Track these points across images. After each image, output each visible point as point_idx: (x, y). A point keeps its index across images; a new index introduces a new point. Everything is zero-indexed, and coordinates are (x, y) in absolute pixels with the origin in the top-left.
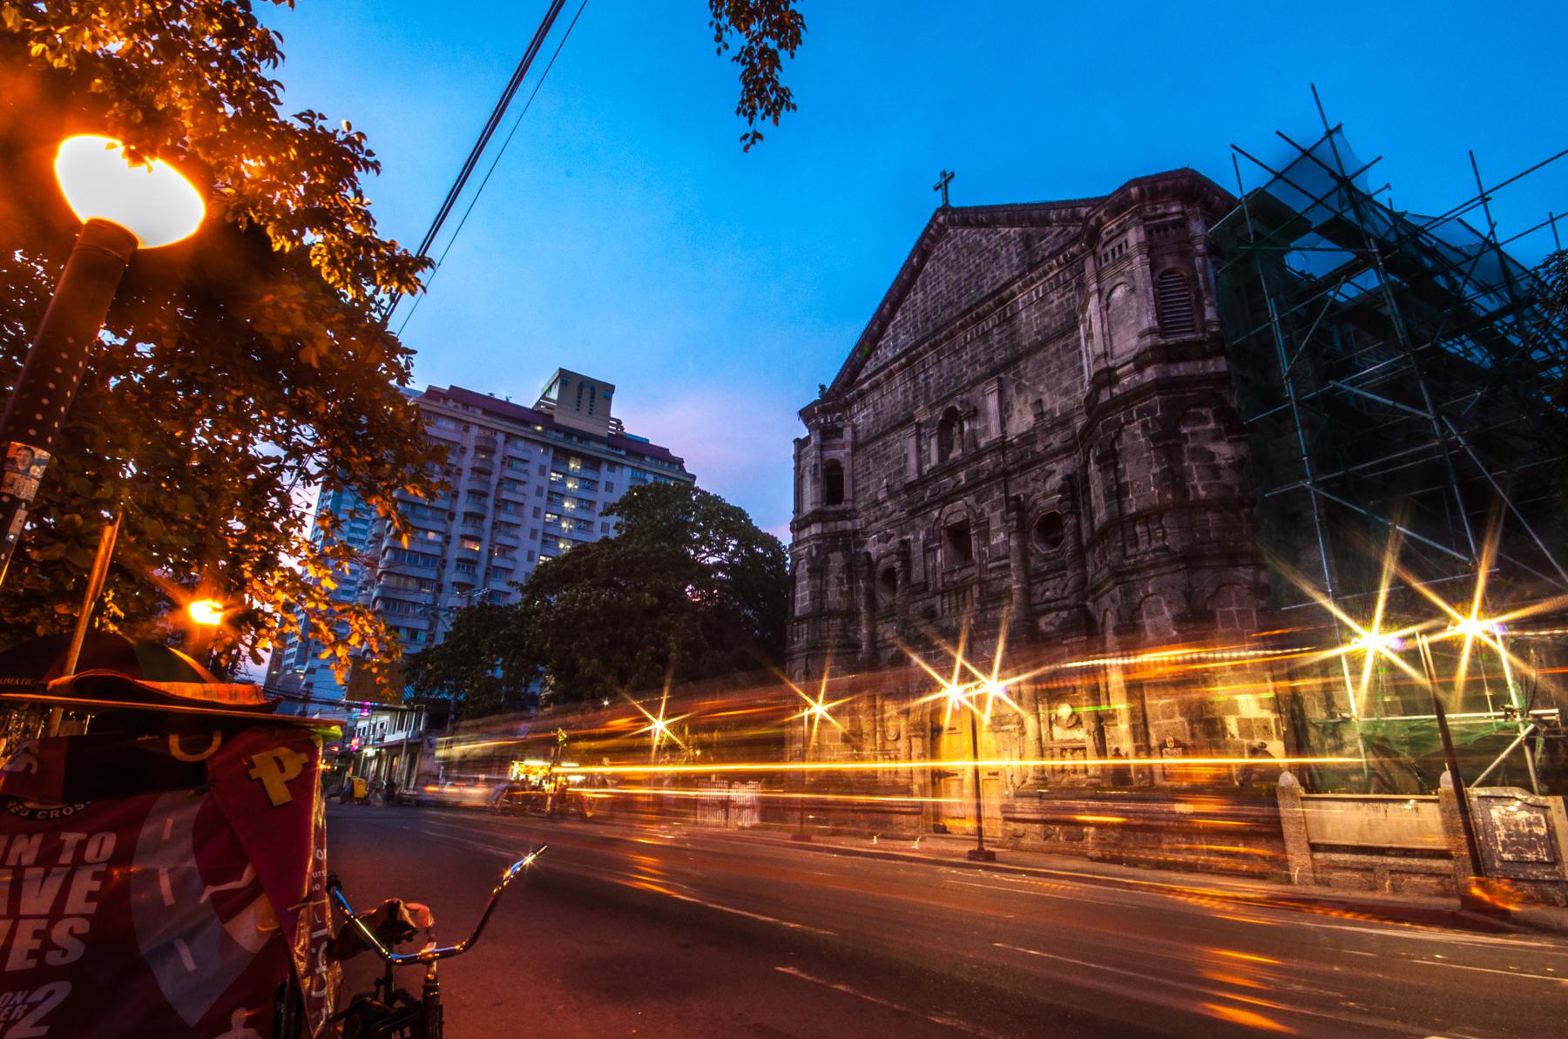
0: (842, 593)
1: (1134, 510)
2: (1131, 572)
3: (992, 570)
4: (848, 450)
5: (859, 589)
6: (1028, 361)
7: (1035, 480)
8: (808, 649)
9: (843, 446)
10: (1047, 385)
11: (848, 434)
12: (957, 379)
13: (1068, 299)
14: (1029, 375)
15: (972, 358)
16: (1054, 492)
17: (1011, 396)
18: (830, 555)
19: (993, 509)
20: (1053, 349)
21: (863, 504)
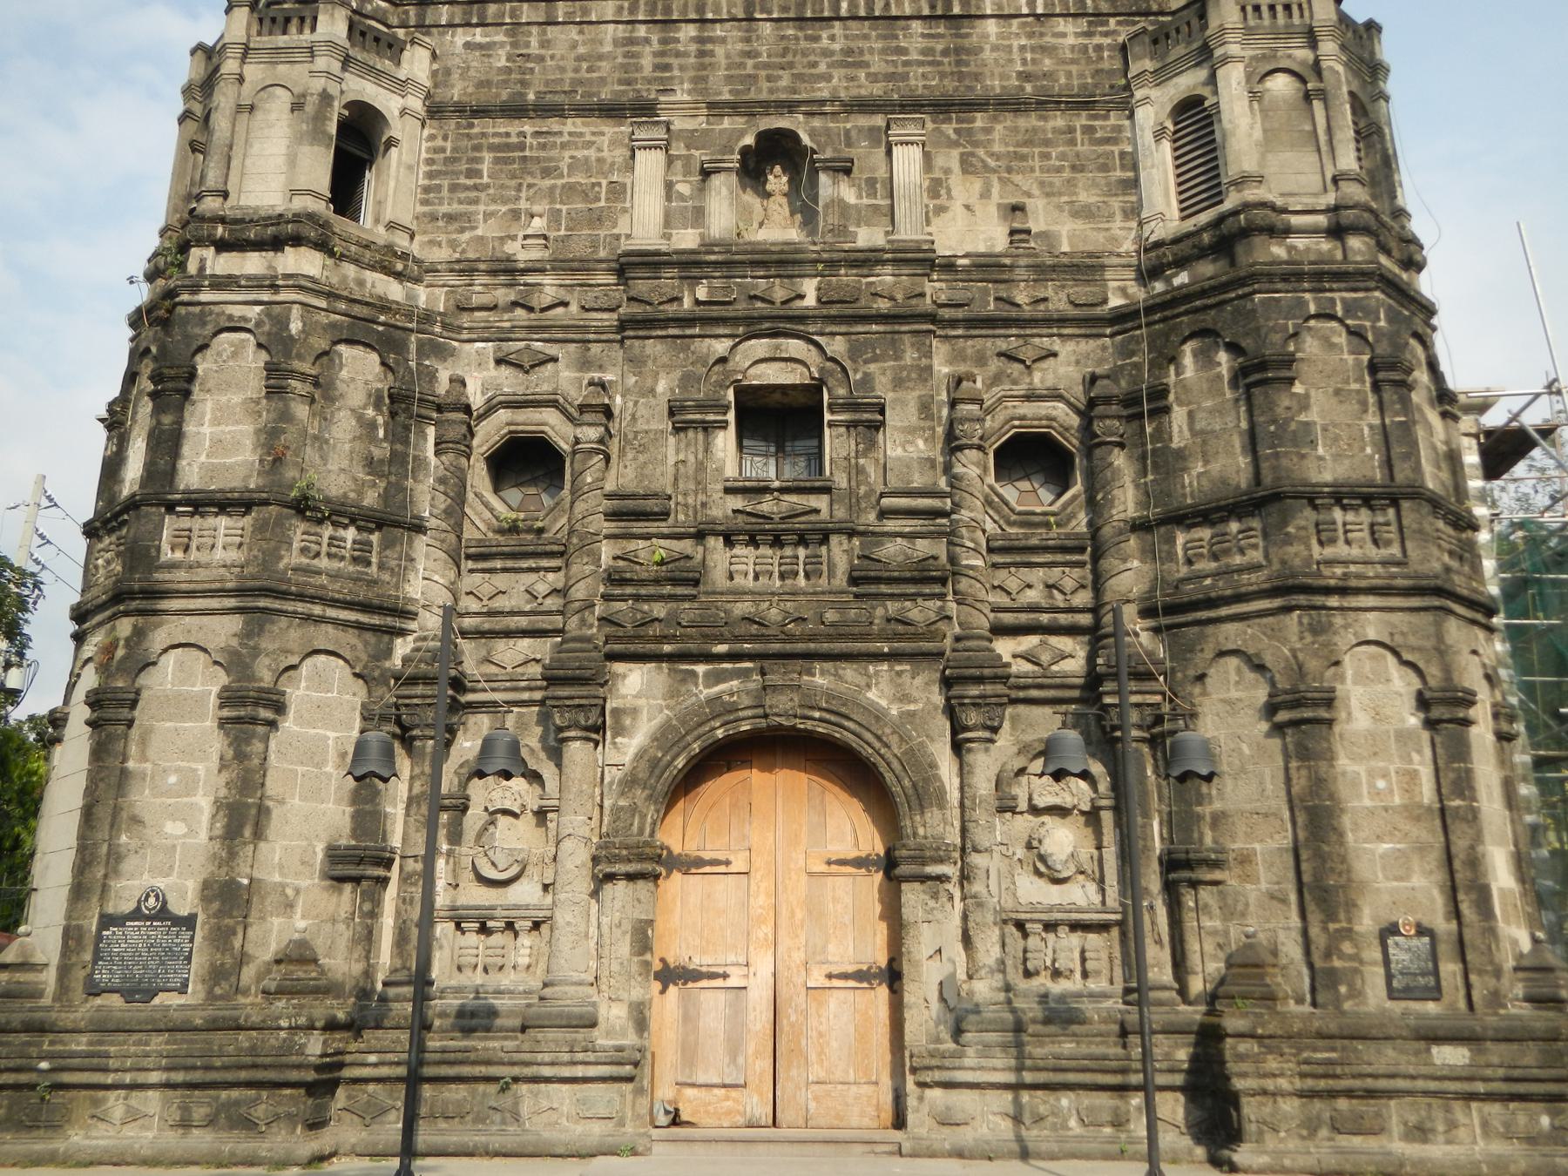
0: (370, 464)
1: (1328, 477)
2: (1328, 591)
3: (884, 514)
4: (416, 103)
5: (420, 462)
6: (995, 119)
7: (1009, 356)
8: (240, 592)
9: (401, 86)
10: (1042, 184)
11: (416, 64)
12: (799, 77)
13: (1099, 48)
14: (997, 148)
15: (849, 52)
16: (1055, 395)
17: (947, 171)
18: (342, 348)
19: (898, 383)
20: (1058, 121)
21: (441, 255)
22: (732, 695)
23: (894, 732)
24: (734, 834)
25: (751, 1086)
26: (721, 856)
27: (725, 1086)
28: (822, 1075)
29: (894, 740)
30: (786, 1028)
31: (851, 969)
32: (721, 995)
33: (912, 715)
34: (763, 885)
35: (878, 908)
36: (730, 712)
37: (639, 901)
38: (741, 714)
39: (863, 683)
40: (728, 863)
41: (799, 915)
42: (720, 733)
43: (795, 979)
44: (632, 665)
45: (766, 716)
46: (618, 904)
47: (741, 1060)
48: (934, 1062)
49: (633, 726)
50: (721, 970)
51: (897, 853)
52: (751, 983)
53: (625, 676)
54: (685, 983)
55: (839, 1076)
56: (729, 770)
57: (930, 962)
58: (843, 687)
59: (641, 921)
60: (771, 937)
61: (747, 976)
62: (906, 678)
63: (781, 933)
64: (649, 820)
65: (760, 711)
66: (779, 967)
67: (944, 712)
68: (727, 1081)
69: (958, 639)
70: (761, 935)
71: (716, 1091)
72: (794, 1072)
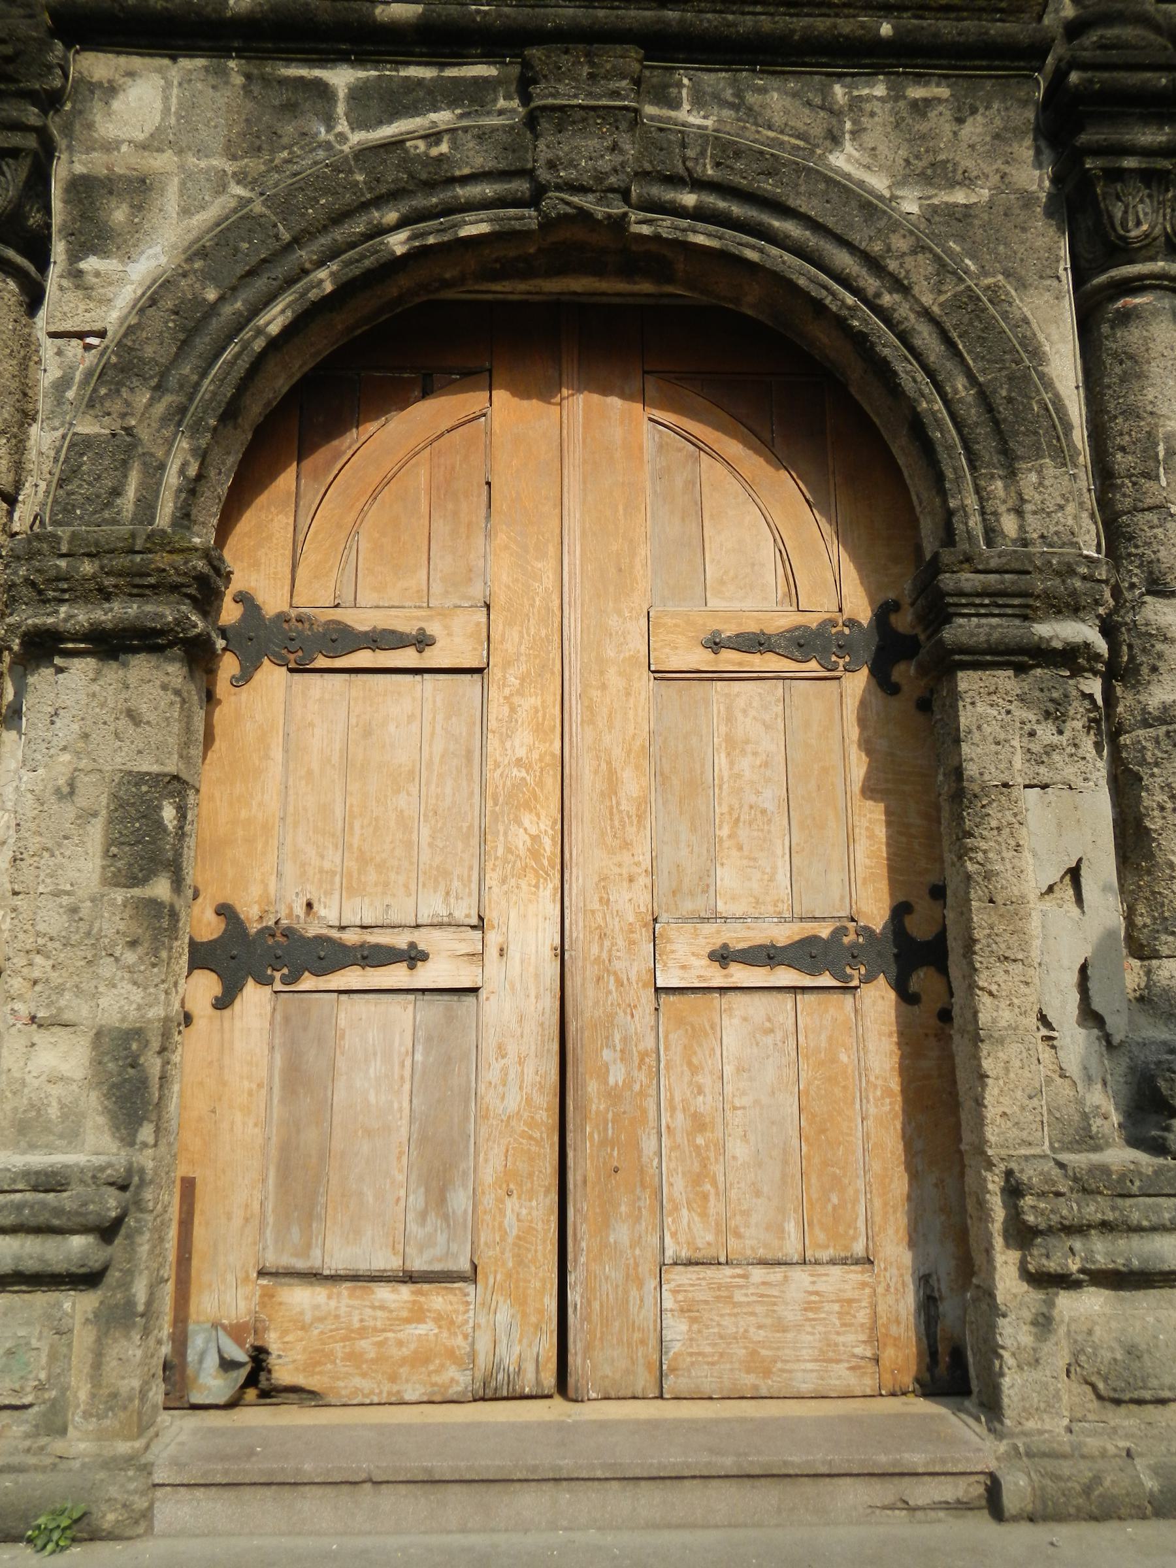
22: (433, 137)
23: (919, 248)
24: (443, 563)
25: (491, 1276)
26: (405, 624)
27: (410, 1278)
28: (705, 1239)
29: (919, 271)
30: (597, 1105)
31: (783, 935)
32: (402, 1012)
33: (963, 215)
34: (527, 703)
35: (859, 766)
36: (430, 186)
37: (133, 717)
38: (463, 192)
39: (817, 131)
40: (422, 642)
41: (631, 785)
42: (398, 243)
43: (618, 965)
44: (136, 62)
45: (533, 201)
46: (68, 729)
47: (460, 1200)
48: (1094, 1210)
49: (136, 228)
50: (400, 940)
51: (947, 581)
52: (492, 975)
53: (111, 90)
54: (289, 980)
55: (753, 1240)
56: (427, 393)
57: (1048, 904)
58: (752, 136)
59: (140, 778)
60: (549, 846)
61: (478, 957)
62: (940, 121)
63: (579, 834)
64: (172, 479)
65: (521, 187)
66: (575, 931)
67: (1050, 213)
68: (418, 1264)
69: (1074, 29)
70: (521, 841)
71: (383, 1293)
72: (621, 1234)
